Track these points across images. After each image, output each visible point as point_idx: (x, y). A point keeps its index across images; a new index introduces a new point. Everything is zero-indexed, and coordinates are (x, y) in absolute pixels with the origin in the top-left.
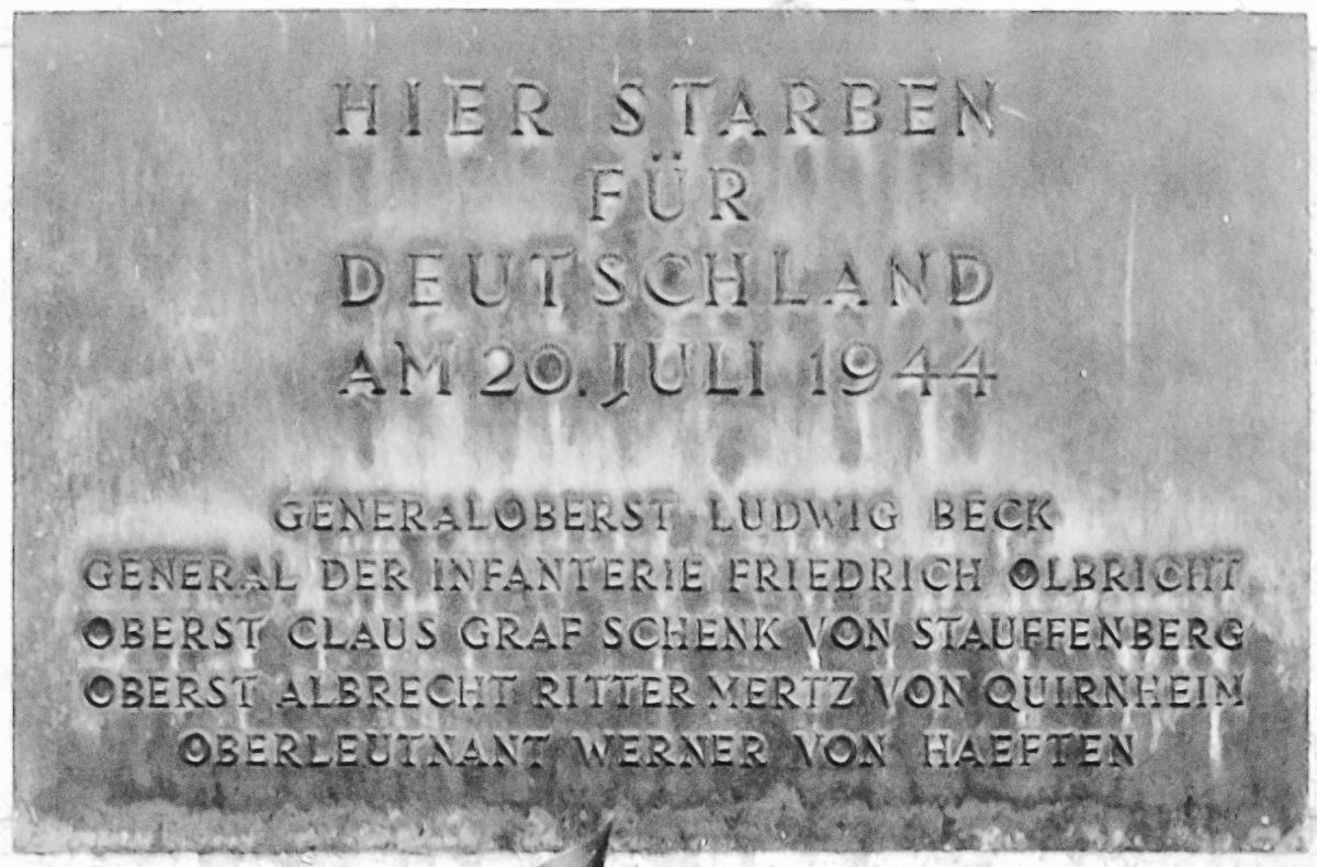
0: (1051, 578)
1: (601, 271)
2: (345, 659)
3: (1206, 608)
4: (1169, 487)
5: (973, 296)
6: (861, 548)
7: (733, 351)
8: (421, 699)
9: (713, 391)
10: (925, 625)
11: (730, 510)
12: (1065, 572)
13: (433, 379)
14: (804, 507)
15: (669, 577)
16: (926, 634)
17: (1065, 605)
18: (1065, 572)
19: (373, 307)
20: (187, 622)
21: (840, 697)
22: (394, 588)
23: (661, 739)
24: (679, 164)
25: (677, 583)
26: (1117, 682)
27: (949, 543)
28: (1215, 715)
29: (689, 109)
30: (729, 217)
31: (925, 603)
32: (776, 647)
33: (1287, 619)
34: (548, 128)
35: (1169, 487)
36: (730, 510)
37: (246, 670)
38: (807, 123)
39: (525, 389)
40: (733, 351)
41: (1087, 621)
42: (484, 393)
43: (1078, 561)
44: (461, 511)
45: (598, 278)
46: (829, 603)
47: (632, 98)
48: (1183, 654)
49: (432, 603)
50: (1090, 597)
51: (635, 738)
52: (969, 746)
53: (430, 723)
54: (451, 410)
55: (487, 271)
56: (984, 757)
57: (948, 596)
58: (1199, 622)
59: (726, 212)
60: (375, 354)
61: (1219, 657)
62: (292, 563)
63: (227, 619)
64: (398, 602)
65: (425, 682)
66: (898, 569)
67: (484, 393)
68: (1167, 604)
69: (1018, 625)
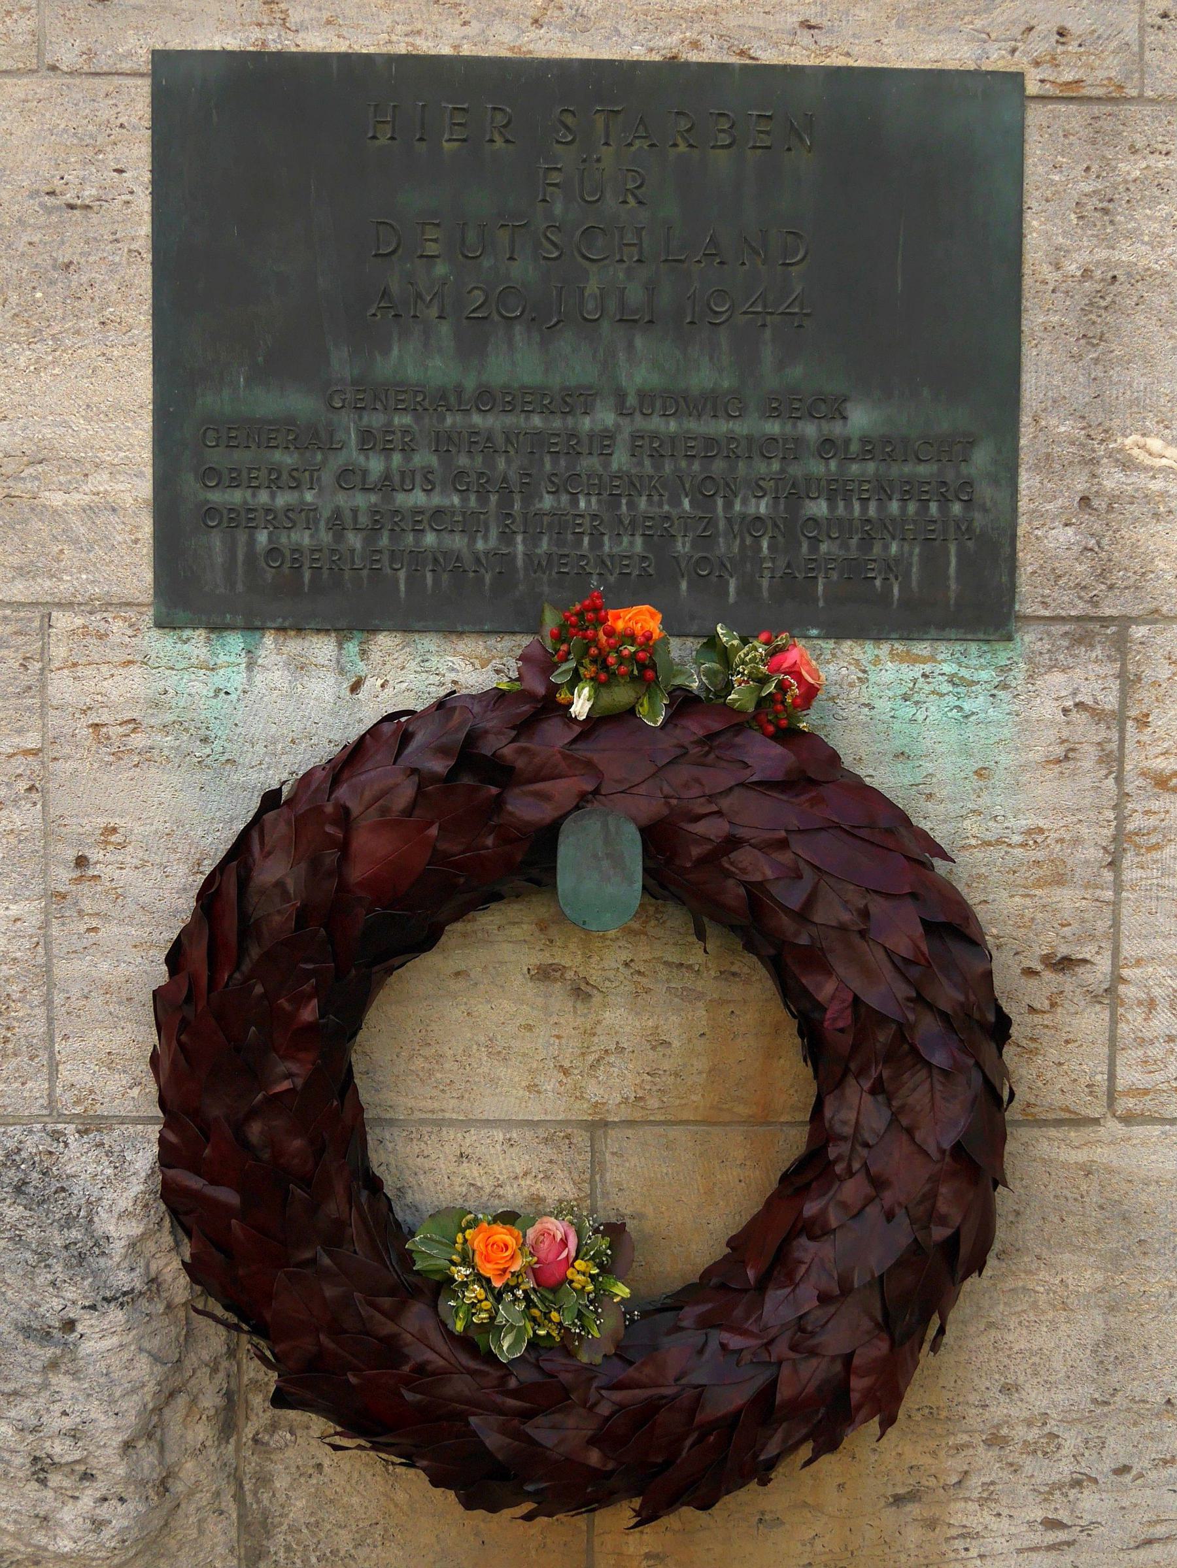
0: (846, 454)
1: (548, 238)
2: (373, 498)
3: (950, 476)
4: (926, 392)
5: (799, 258)
6: (722, 427)
7: (635, 294)
8: (425, 525)
9: (621, 320)
10: (761, 483)
11: (632, 400)
12: (854, 447)
13: (434, 312)
14: (681, 401)
15: (591, 448)
16: (761, 487)
17: (855, 468)
18: (854, 447)
19: (394, 258)
20: (270, 471)
21: (704, 530)
22: (408, 450)
23: (583, 557)
24: (601, 166)
25: (596, 452)
26: (888, 522)
27: (773, 428)
28: (953, 549)
29: (607, 127)
30: (632, 201)
31: (761, 467)
32: (661, 495)
33: (1003, 482)
34: (510, 138)
35: (926, 392)
36: (632, 400)
37: (309, 504)
38: (685, 139)
39: (496, 317)
40: (635, 294)
41: (869, 482)
42: (468, 318)
43: (864, 440)
44: (453, 399)
45: (544, 241)
46: (696, 467)
47: (569, 120)
48: (934, 507)
49: (434, 461)
50: (871, 467)
51: (567, 556)
52: (788, 566)
53: (430, 539)
54: (445, 328)
55: (471, 236)
56: (799, 572)
57: (776, 466)
58: (944, 483)
59: (630, 199)
60: (395, 288)
61: (957, 508)
62: (340, 435)
63: (296, 470)
64: (407, 459)
65: (428, 515)
66: (744, 443)
67: (468, 318)
68: (923, 470)
69: (823, 483)
